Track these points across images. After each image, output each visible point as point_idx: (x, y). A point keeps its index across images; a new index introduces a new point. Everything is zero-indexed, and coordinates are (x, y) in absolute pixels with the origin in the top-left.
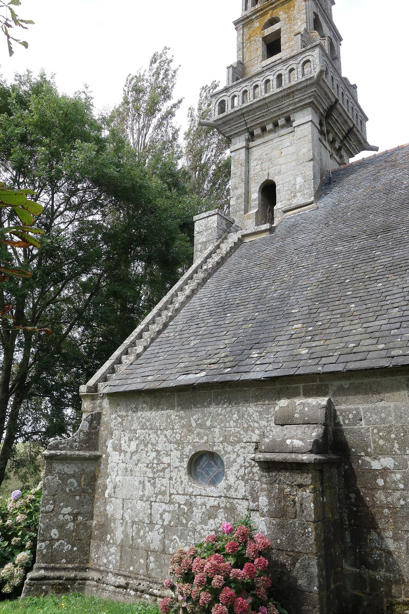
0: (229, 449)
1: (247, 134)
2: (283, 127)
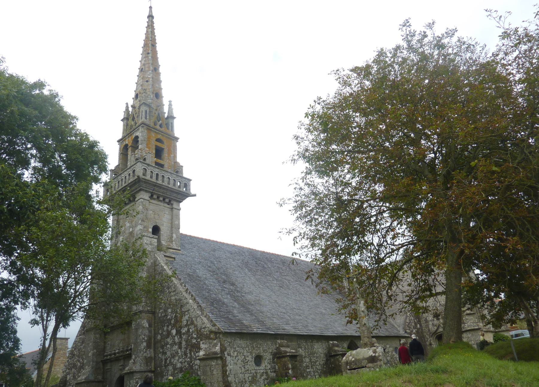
0: (265, 354)
1: (150, 194)
2: (166, 203)
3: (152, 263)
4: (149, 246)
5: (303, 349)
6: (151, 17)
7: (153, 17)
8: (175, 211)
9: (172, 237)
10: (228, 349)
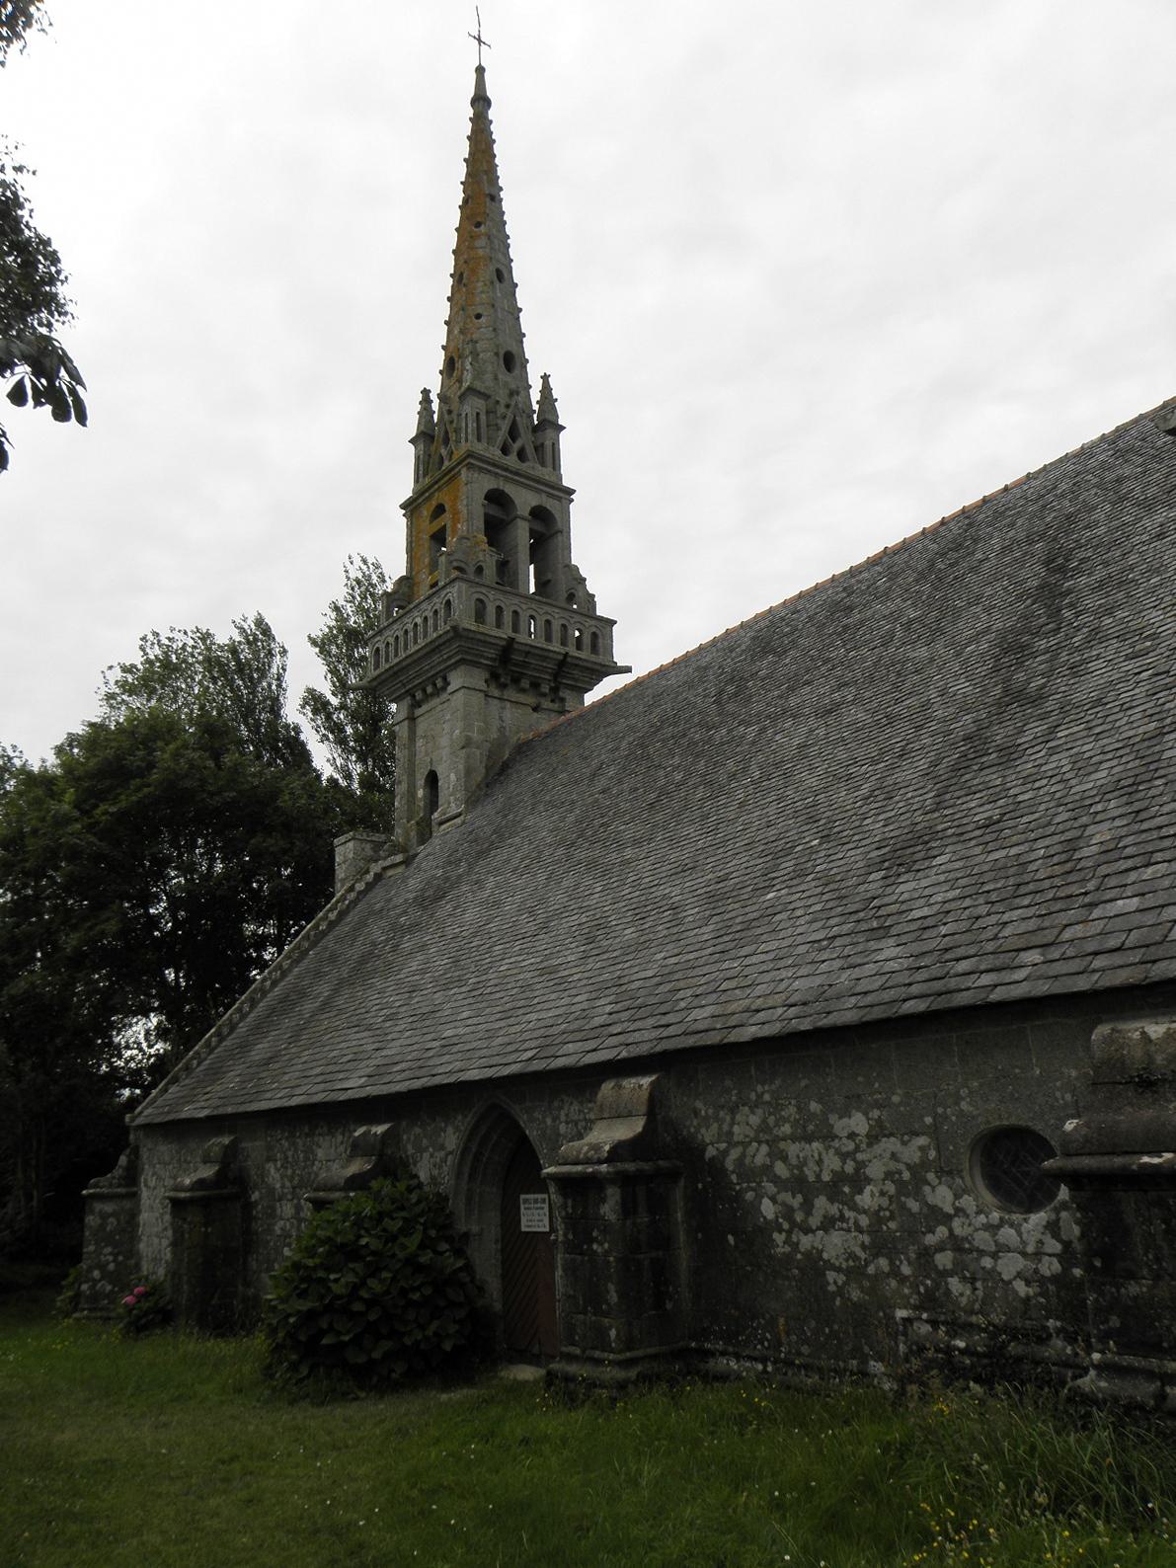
6: (481, 101)
7: (487, 103)
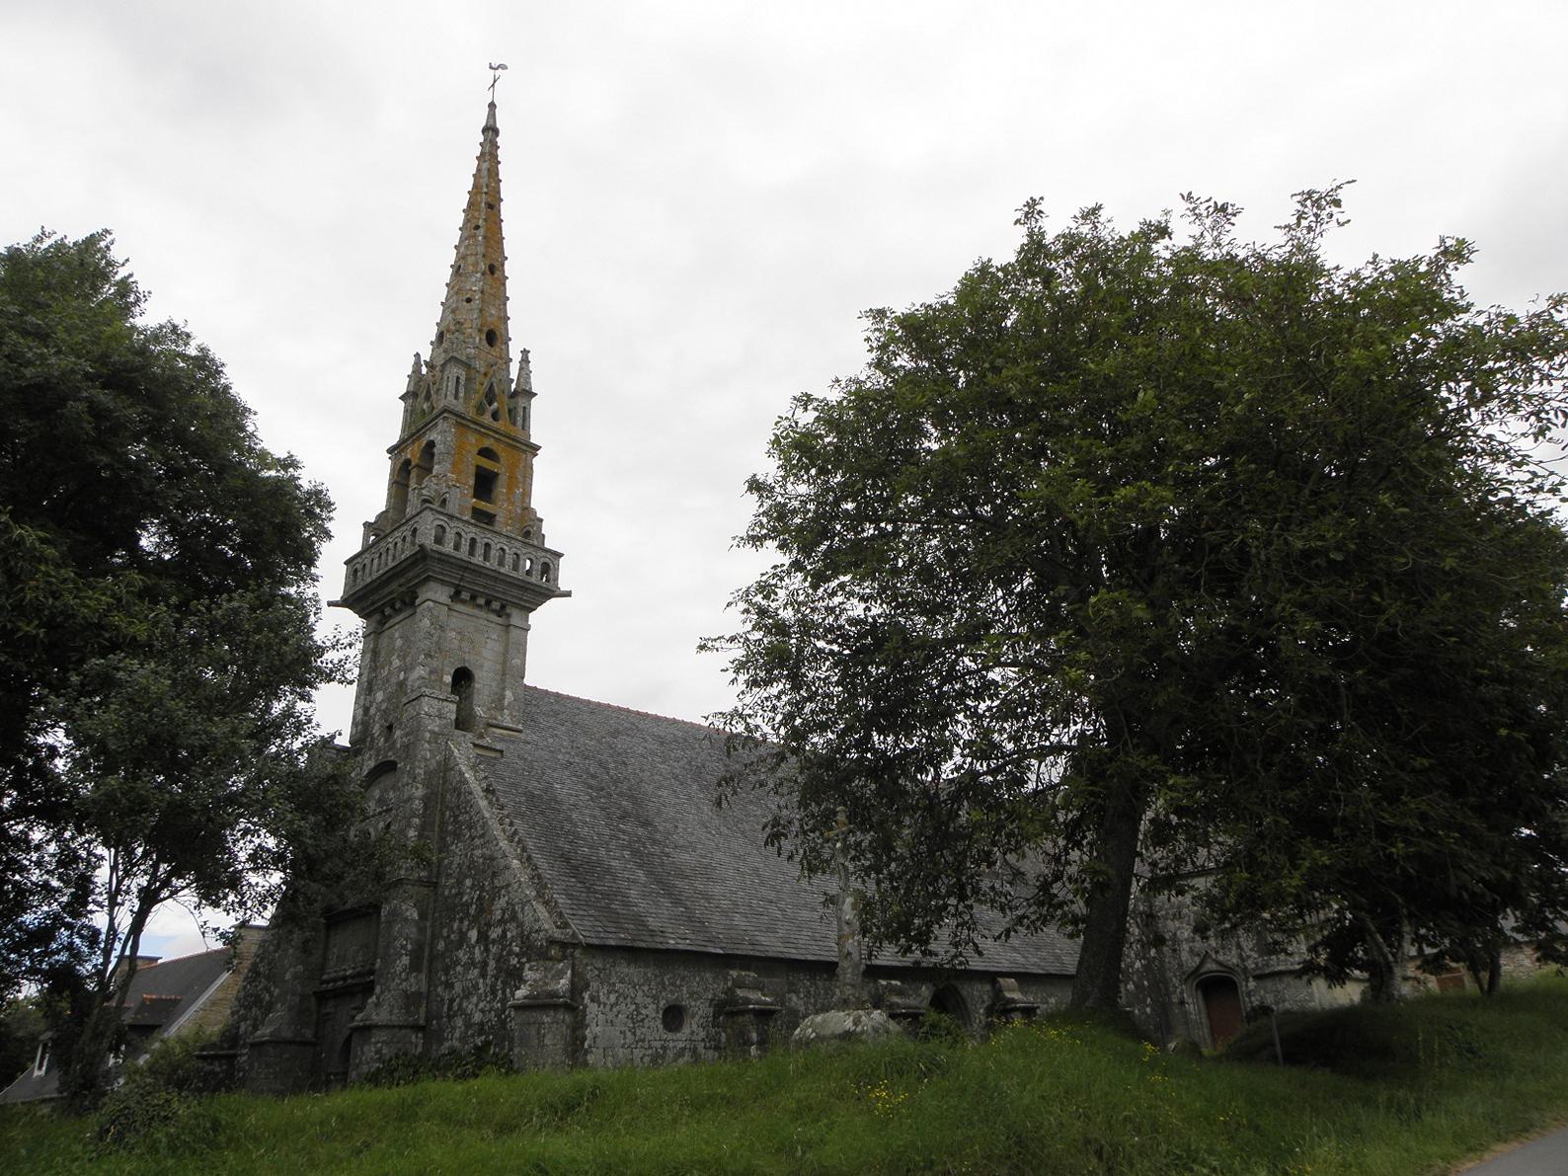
0: (693, 1003)
2: (494, 611)
3: (439, 763)
4: (434, 721)
5: (802, 995)
6: (491, 130)
7: (496, 132)
8: (514, 633)
9: (503, 697)
10: (594, 985)
